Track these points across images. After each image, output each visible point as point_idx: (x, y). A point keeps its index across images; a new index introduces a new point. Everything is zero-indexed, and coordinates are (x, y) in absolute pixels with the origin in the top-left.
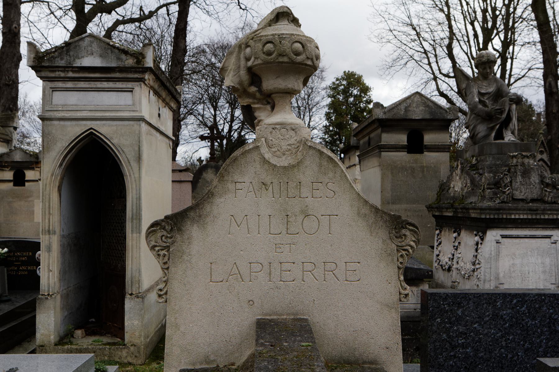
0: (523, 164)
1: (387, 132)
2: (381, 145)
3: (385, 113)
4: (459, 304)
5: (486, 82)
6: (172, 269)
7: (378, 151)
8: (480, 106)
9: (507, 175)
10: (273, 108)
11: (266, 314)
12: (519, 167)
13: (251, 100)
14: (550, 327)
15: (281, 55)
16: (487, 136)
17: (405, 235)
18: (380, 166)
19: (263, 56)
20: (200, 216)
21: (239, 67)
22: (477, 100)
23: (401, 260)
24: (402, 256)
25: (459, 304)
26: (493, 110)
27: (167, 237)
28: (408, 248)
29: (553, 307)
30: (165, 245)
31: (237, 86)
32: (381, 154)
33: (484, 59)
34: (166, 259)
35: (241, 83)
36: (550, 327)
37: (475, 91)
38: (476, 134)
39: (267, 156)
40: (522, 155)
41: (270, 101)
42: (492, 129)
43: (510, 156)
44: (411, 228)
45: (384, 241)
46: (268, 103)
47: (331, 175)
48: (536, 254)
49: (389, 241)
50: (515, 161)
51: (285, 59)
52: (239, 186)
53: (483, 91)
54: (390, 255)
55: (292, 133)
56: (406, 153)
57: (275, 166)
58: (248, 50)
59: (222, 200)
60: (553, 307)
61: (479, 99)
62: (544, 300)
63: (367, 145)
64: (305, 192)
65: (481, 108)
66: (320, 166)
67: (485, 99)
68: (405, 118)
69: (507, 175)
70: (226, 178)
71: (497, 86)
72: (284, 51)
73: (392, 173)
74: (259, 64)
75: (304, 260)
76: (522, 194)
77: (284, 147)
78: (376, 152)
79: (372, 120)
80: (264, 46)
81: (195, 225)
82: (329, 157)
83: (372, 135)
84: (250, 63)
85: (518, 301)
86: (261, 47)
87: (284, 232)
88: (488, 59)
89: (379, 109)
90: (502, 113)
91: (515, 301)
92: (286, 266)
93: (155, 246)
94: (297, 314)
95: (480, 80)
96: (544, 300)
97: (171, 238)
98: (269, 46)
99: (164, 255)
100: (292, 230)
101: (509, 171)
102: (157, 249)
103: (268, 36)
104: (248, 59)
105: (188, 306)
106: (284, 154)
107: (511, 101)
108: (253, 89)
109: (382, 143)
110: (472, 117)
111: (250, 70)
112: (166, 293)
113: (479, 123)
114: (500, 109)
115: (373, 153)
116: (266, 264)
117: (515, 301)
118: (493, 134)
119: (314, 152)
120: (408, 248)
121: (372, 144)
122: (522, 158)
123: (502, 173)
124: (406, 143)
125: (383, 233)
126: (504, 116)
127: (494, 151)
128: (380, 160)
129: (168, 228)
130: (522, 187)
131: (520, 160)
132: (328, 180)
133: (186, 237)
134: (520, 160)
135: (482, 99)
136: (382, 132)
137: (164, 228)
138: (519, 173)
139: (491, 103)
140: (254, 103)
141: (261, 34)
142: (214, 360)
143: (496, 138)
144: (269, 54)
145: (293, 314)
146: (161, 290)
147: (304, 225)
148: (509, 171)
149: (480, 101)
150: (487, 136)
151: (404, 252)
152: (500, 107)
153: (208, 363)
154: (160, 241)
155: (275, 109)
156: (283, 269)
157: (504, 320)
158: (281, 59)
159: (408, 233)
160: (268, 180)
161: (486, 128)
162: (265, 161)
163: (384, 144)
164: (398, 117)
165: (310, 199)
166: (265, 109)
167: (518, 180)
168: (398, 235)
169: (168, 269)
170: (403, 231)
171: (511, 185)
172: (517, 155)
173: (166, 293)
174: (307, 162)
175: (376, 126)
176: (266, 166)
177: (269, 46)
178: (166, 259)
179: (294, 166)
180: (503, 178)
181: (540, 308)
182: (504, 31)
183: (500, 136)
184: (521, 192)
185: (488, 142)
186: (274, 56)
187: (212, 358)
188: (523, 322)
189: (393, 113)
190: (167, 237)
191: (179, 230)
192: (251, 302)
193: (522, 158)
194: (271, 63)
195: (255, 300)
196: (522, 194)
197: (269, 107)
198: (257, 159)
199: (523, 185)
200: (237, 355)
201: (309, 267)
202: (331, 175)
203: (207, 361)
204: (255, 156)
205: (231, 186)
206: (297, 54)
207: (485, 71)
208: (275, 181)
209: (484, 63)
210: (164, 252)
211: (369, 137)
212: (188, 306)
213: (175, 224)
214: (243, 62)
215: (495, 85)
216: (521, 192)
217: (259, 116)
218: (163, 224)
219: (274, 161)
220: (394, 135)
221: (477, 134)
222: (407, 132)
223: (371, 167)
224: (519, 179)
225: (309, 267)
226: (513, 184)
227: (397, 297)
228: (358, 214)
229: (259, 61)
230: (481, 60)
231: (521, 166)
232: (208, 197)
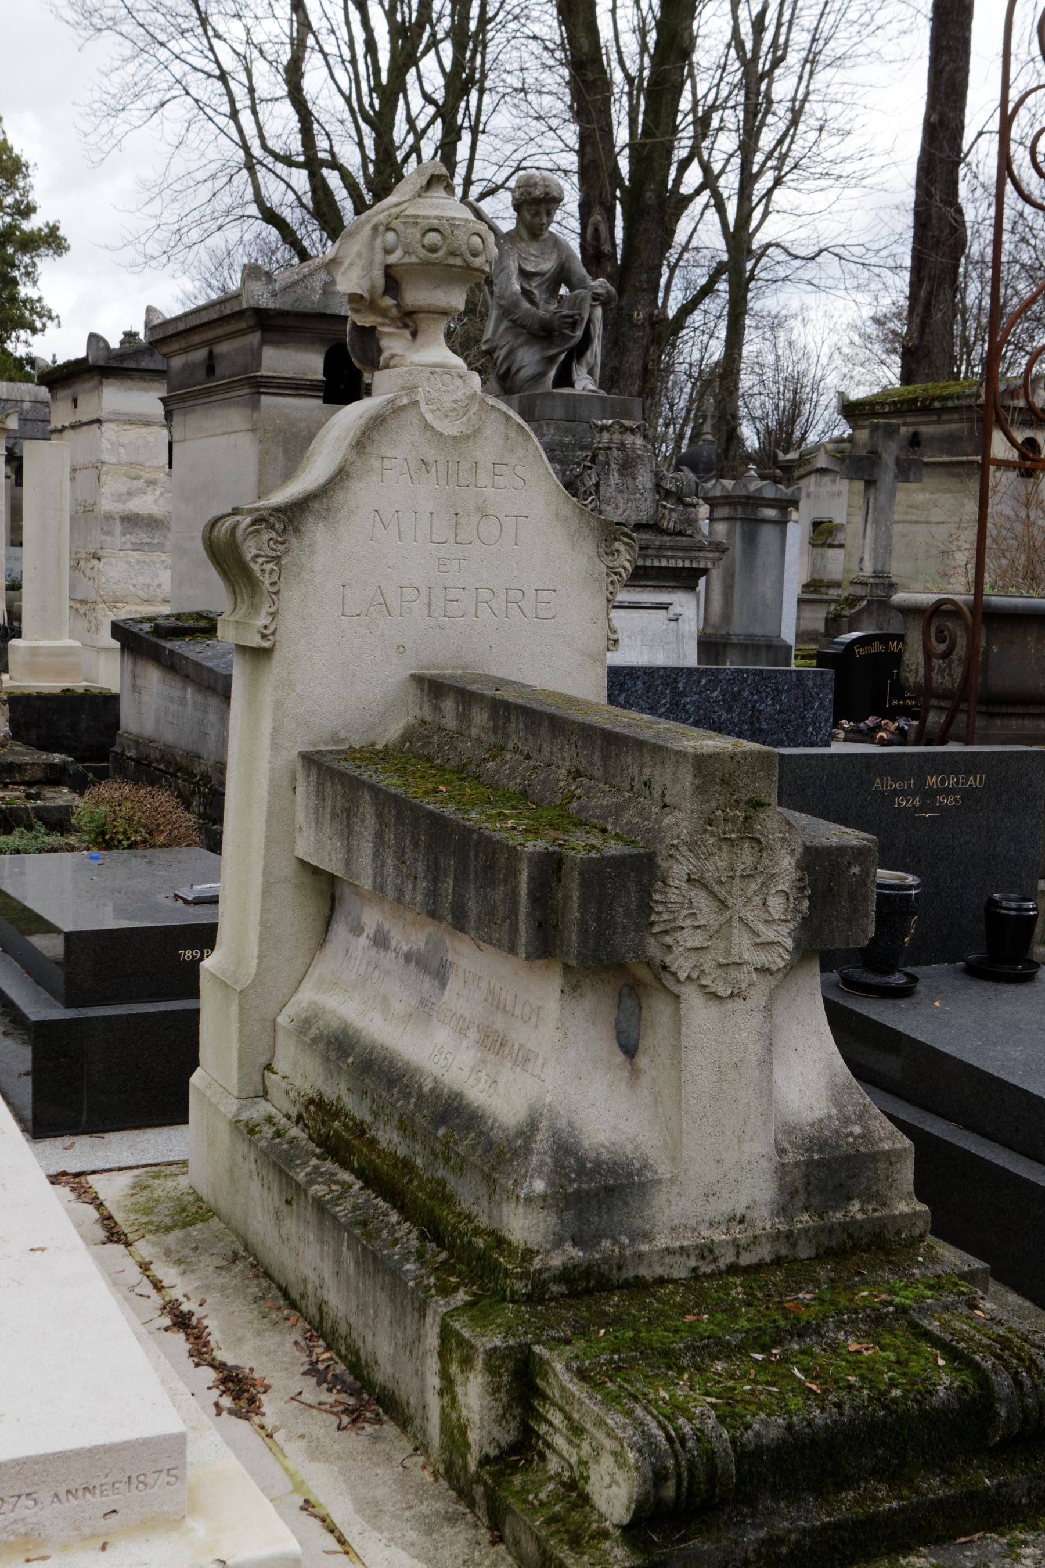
0: (622, 446)
1: (277, 344)
2: (262, 377)
3: (274, 294)
4: (622, 685)
5: (535, 245)
6: (285, 594)
7: (247, 391)
8: (526, 305)
9: (590, 468)
10: (414, 335)
11: (423, 667)
12: (615, 453)
13: (380, 320)
14: (752, 724)
15: (452, 254)
16: (539, 377)
17: (618, 551)
18: (253, 430)
19: (422, 252)
20: (328, 510)
21: (371, 263)
22: (517, 287)
23: (611, 588)
24: (612, 582)
25: (622, 685)
26: (557, 316)
27: (277, 542)
28: (621, 570)
29: (758, 691)
30: (273, 554)
31: (366, 295)
32: (259, 401)
33: (537, 193)
34: (275, 576)
35: (372, 289)
36: (752, 724)
37: (513, 266)
38: (514, 369)
39: (429, 417)
40: (622, 426)
41: (410, 323)
42: (551, 360)
43: (597, 426)
44: (626, 540)
45: (590, 559)
46: (406, 326)
47: (520, 453)
48: (639, 643)
49: (597, 560)
50: (606, 436)
51: (458, 261)
52: (387, 463)
53: (529, 268)
54: (597, 580)
55: (459, 382)
56: (320, 402)
57: (441, 434)
58: (391, 236)
59: (362, 485)
60: (758, 691)
61: (522, 288)
62: (746, 679)
63: (201, 374)
64: (484, 478)
65: (528, 310)
66: (507, 437)
67: (533, 286)
68: (324, 311)
69: (590, 468)
70: (369, 450)
71: (560, 258)
72: (459, 249)
73: (286, 451)
74: (411, 264)
75: (478, 585)
76: (620, 512)
77: (446, 404)
78: (242, 392)
79: (237, 309)
80: (423, 235)
81: (321, 524)
82: (519, 425)
83: (222, 348)
84: (392, 259)
85: (709, 681)
86: (419, 236)
87: (452, 540)
88: (547, 194)
89: (259, 283)
90: (574, 325)
91: (703, 682)
92: (453, 593)
93: (258, 556)
94: (467, 668)
95: (522, 239)
96: (746, 679)
97: (283, 543)
98: (433, 238)
99: (272, 571)
100: (463, 537)
101: (593, 460)
102: (260, 560)
103: (428, 218)
104: (388, 252)
105: (309, 653)
106: (446, 416)
107: (594, 299)
108: (388, 302)
109: (263, 373)
110: (502, 327)
111: (388, 269)
112: (273, 633)
113: (521, 346)
114: (571, 316)
115: (229, 395)
116: (424, 589)
117: (703, 682)
118: (552, 374)
119: (498, 415)
120: (621, 570)
121: (220, 370)
122: (621, 433)
123: (578, 464)
124: (320, 377)
125: (589, 547)
126: (579, 333)
127: (559, 412)
128: (255, 416)
129: (279, 526)
130: (619, 497)
131: (616, 437)
132: (516, 462)
133: (306, 542)
134: (616, 437)
135: (527, 286)
136: (264, 342)
137: (272, 527)
138: (614, 466)
139: (544, 296)
140: (383, 325)
141: (407, 213)
142: (346, 739)
143: (559, 382)
144: (433, 249)
145: (462, 668)
146: (266, 627)
147: (481, 530)
148: (593, 460)
149: (526, 293)
150: (539, 377)
151: (615, 577)
152: (571, 312)
153: (336, 743)
154: (265, 546)
155: (419, 336)
156: (449, 597)
157: (687, 712)
158: (451, 261)
159: (622, 548)
160: (430, 457)
161: (537, 357)
162: (427, 426)
163: (270, 374)
164: (307, 307)
165: (489, 490)
166: (401, 336)
167: (612, 482)
168: (608, 550)
169: (277, 593)
170: (617, 545)
171: (597, 492)
172: (611, 426)
173: (273, 633)
174: (488, 431)
175: (243, 325)
176: (428, 434)
177: (433, 238)
178: (275, 576)
179: (468, 437)
180: (581, 474)
181: (739, 692)
182: (617, 150)
183: (565, 379)
184: (617, 507)
185: (541, 391)
186: (440, 254)
187: (343, 734)
188: (714, 716)
189: (294, 296)
190: (277, 542)
191: (297, 530)
192: (401, 648)
193: (621, 433)
194: (434, 264)
195: (407, 646)
196: (620, 512)
197: (407, 333)
198: (416, 421)
199: (621, 492)
200: (379, 730)
201: (485, 595)
202: (520, 453)
203: (336, 740)
204: (411, 416)
205: (375, 463)
206: (475, 254)
207: (536, 220)
208: (441, 459)
209: (536, 202)
210: (271, 566)
211: (211, 354)
212: (309, 653)
213: (290, 521)
214: (379, 256)
215: (554, 256)
216: (617, 507)
217: (389, 348)
218: (272, 520)
219: (437, 425)
220: (293, 354)
221: (518, 371)
222: (325, 350)
223: (219, 431)
224: (614, 477)
225: (485, 595)
226: (602, 489)
227: (604, 643)
228: (557, 515)
229: (413, 259)
230: (529, 193)
231: (618, 449)
232: (342, 479)
